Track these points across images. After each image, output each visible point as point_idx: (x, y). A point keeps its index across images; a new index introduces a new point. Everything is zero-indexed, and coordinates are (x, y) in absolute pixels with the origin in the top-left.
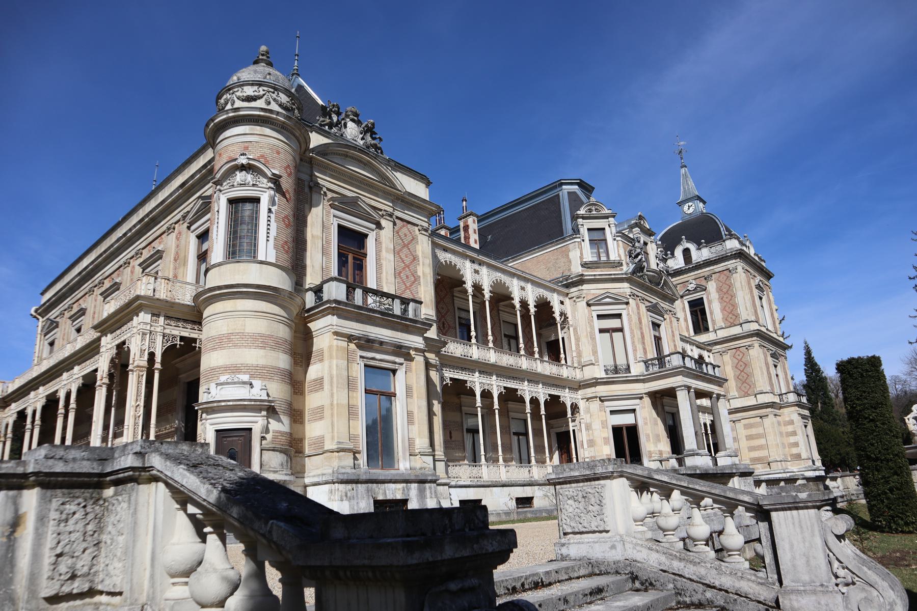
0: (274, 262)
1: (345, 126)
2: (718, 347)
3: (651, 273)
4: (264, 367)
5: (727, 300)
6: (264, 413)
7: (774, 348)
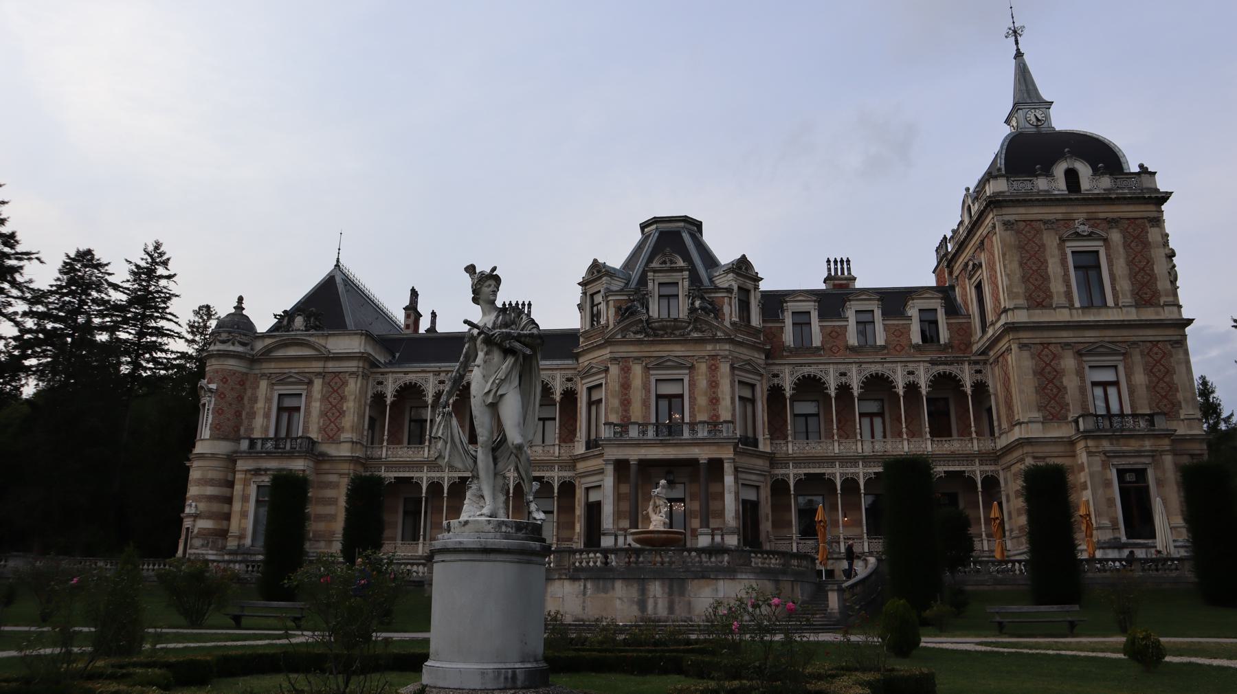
0: (208, 437)
1: (293, 321)
2: (991, 353)
3: (656, 324)
4: (198, 496)
5: (993, 279)
6: (192, 519)
7: (1090, 336)
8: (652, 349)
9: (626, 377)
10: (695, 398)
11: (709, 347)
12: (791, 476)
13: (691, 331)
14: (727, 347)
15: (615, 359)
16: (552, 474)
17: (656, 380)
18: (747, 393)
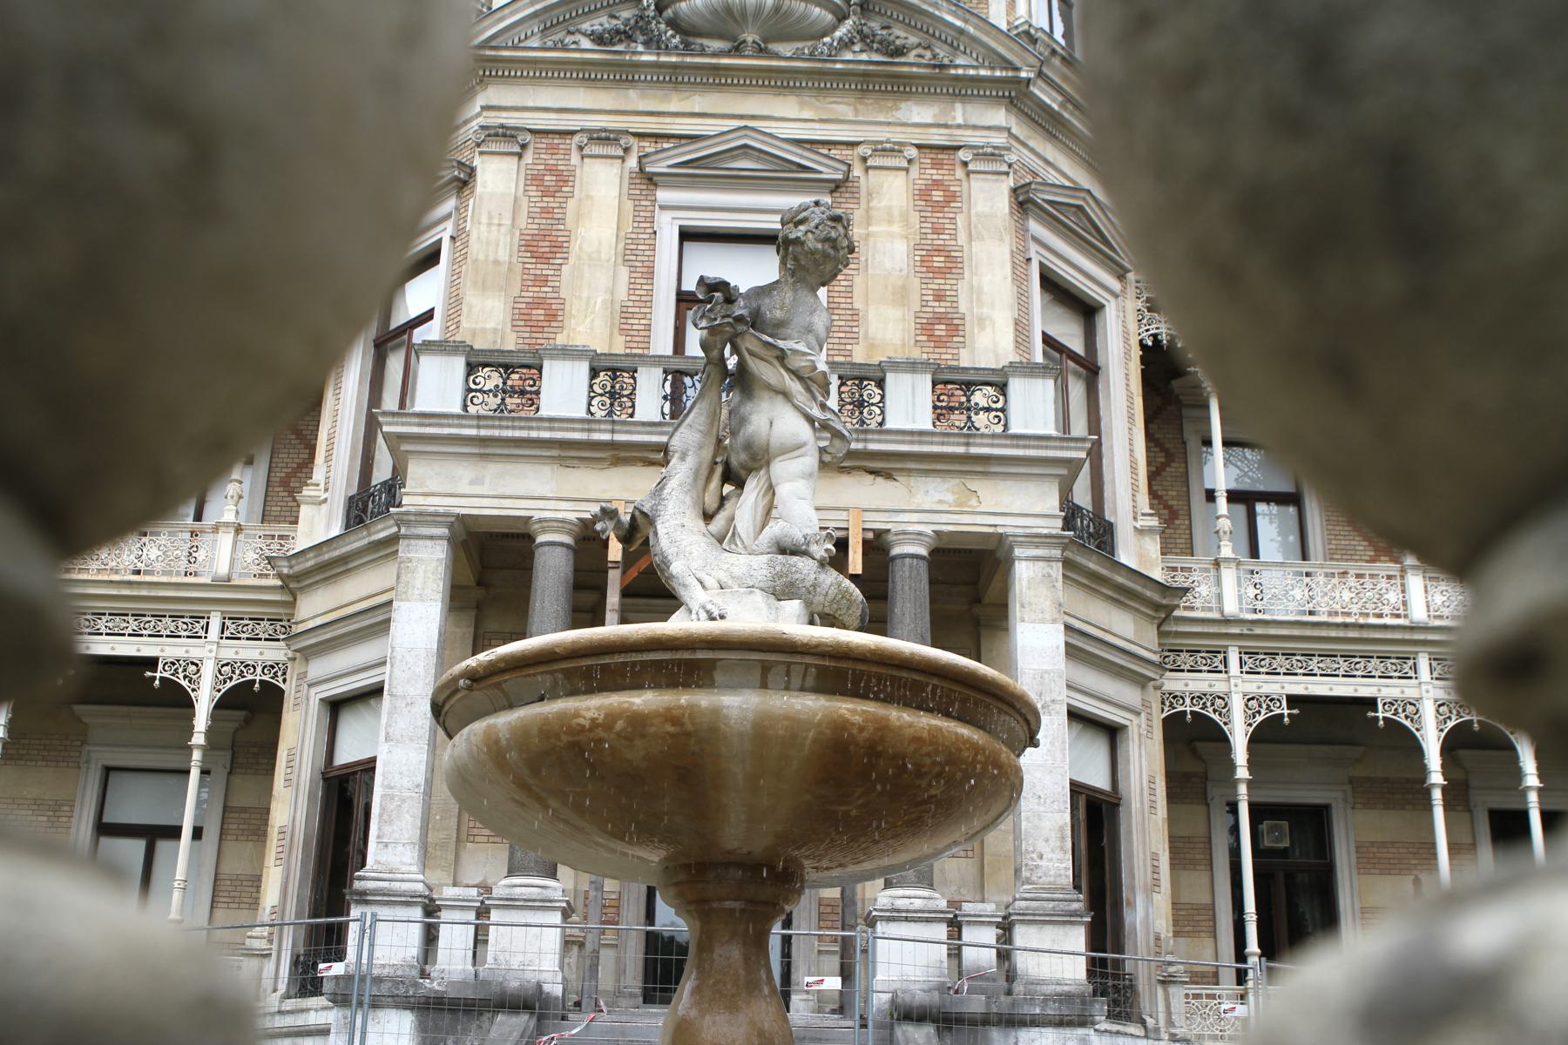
8: (673, 107)
9: (546, 211)
10: (855, 313)
11: (919, 113)
12: (1237, 705)
13: (846, 44)
14: (999, 116)
15: (505, 133)
16: (195, 650)
17: (688, 236)
18: (1071, 335)
